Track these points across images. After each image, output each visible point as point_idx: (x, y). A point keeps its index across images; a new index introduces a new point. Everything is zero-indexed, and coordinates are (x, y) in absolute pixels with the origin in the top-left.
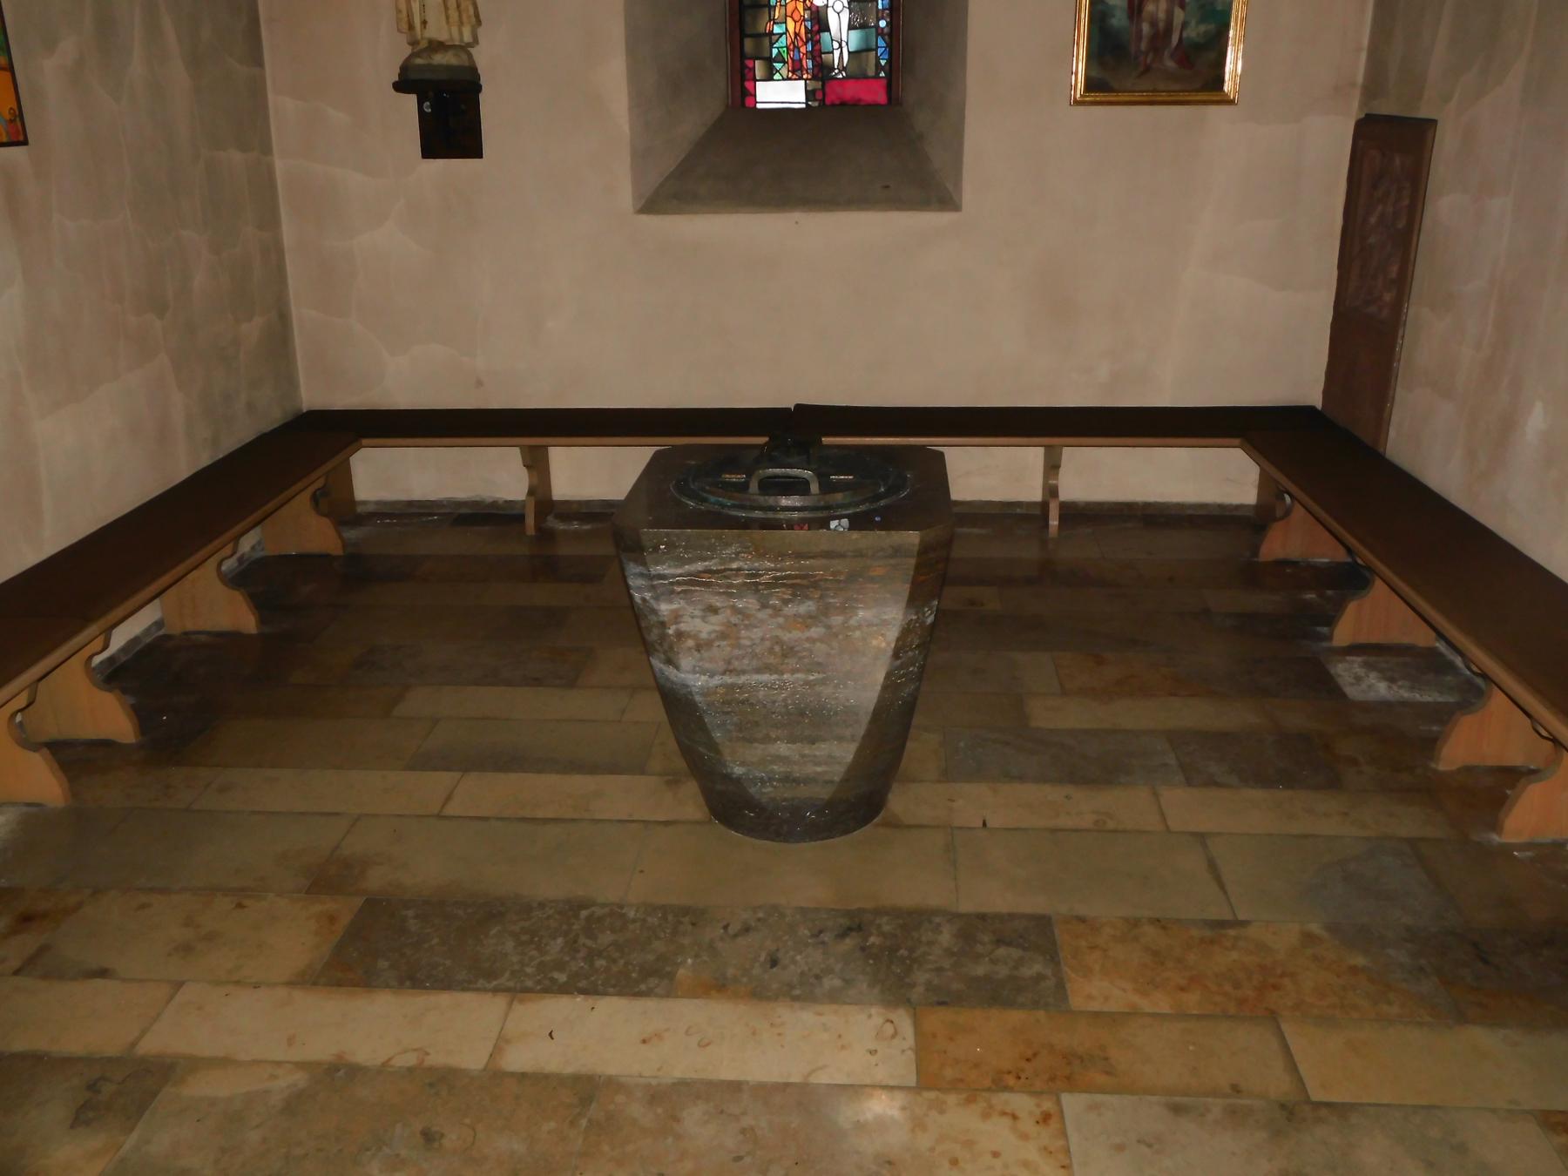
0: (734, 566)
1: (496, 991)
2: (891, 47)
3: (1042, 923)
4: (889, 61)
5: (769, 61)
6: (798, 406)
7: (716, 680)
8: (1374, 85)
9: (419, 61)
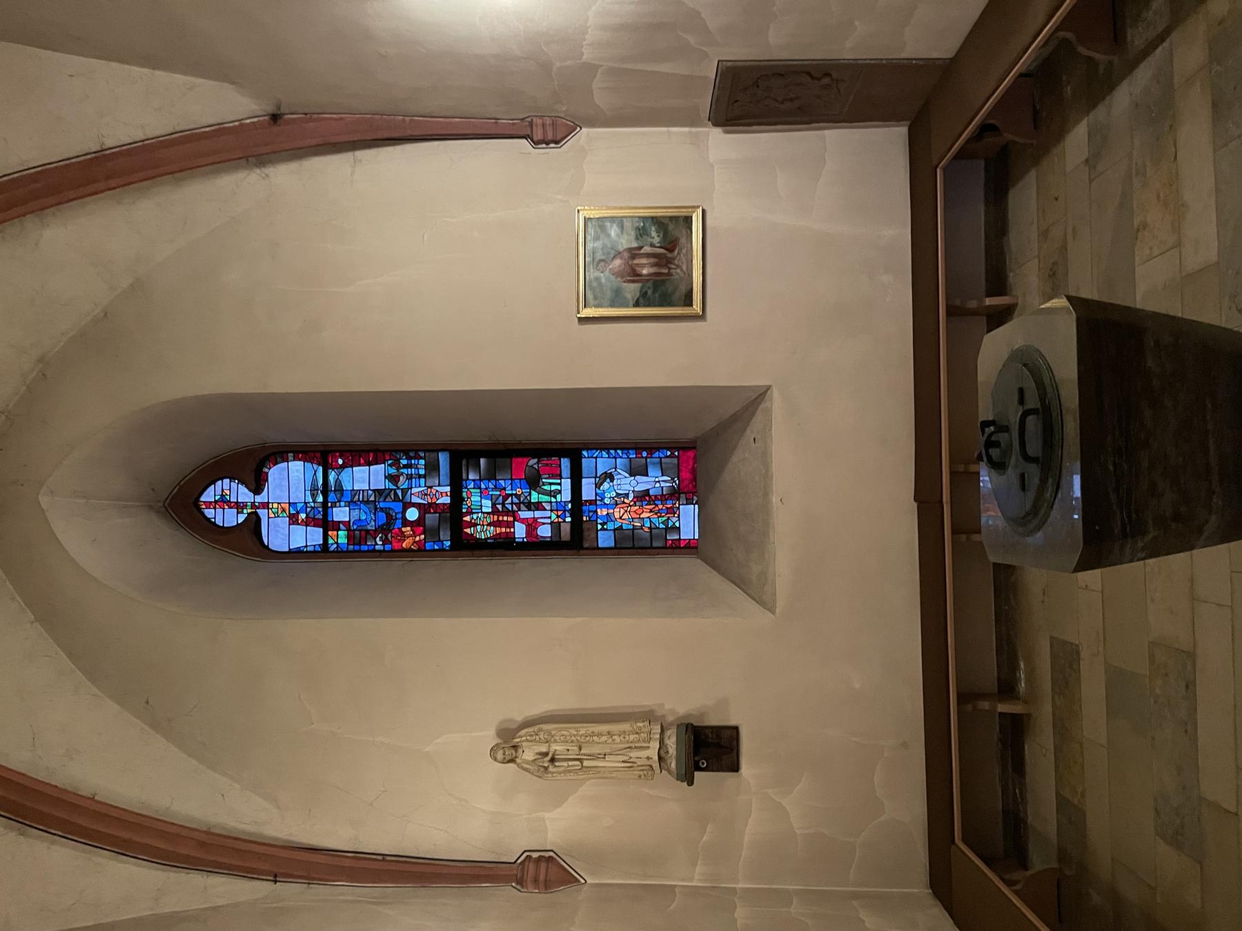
0: (1111, 468)
2: (658, 449)
4: (668, 449)
5: (667, 529)
6: (916, 498)
9: (673, 765)
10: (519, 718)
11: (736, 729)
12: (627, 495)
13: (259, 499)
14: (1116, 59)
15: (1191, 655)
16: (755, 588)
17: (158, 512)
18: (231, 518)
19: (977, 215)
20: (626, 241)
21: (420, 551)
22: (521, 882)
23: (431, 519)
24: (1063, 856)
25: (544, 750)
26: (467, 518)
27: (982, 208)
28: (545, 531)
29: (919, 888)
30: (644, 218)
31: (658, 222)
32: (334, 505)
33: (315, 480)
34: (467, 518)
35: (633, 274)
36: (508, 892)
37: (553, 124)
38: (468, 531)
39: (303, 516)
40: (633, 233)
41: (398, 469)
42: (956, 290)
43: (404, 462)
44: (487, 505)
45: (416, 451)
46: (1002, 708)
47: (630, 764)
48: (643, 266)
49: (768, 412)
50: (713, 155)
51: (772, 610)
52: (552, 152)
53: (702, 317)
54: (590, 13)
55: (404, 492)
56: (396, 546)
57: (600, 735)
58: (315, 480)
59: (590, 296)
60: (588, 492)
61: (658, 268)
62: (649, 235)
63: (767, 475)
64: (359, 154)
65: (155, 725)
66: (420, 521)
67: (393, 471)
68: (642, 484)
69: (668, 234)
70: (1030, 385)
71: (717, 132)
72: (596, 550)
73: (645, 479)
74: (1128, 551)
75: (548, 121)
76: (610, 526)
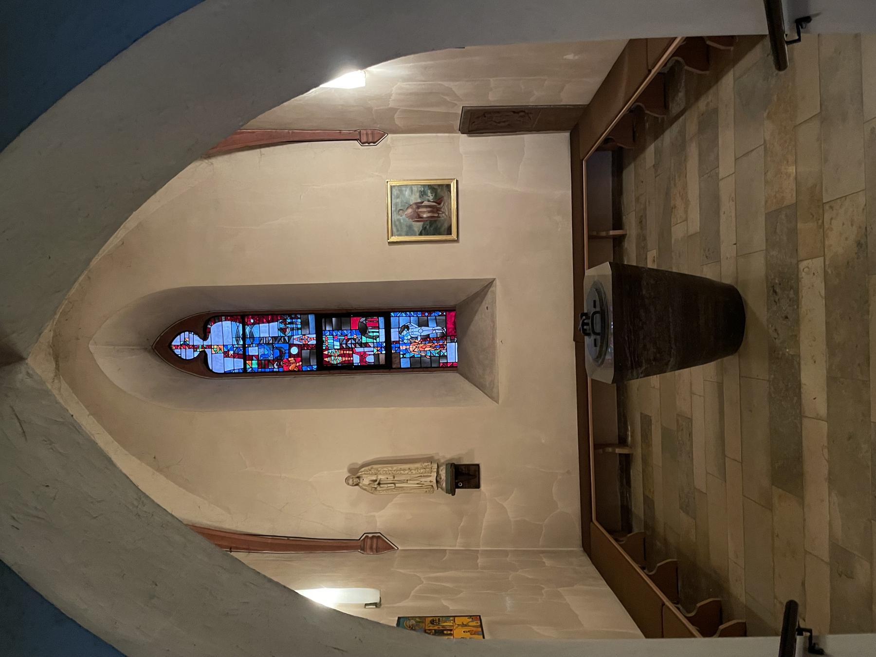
1: (801, 424)
2: (434, 311)
3: (768, 216)
7: (674, 346)
8: (450, 130)
9: (444, 485)
10: (360, 462)
11: (478, 465)
12: (417, 338)
13: (206, 343)
14: (665, 117)
15: (691, 420)
16: (487, 389)
17: (149, 352)
18: (189, 354)
19: (608, 183)
20: (415, 198)
21: (299, 372)
22: (363, 549)
23: (306, 353)
24: (646, 526)
25: (374, 478)
26: (326, 353)
27: (611, 179)
28: (370, 359)
29: (576, 547)
30: (424, 186)
31: (432, 188)
32: (249, 346)
33: (238, 332)
34: (326, 353)
35: (418, 217)
36: (358, 554)
37: (373, 134)
38: (326, 359)
39: (231, 352)
40: (418, 194)
41: (285, 324)
42: (598, 225)
43: (289, 321)
44: (337, 345)
45: (296, 314)
46: (618, 451)
47: (421, 486)
48: (424, 212)
49: (494, 293)
50: (461, 150)
51: (497, 402)
52: (372, 148)
53: (457, 241)
54: (394, 89)
55: (289, 338)
56: (286, 369)
57: (404, 470)
58: (238, 332)
59: (394, 230)
60: (394, 337)
61: (433, 214)
62: (427, 195)
63: (494, 327)
64: (263, 150)
65: (159, 470)
66: (299, 355)
67: (282, 326)
68: (426, 331)
69: (439, 192)
70: (597, 299)
71: (464, 136)
72: (400, 369)
73: (427, 328)
74: (635, 373)
75: (370, 132)
76: (408, 355)
